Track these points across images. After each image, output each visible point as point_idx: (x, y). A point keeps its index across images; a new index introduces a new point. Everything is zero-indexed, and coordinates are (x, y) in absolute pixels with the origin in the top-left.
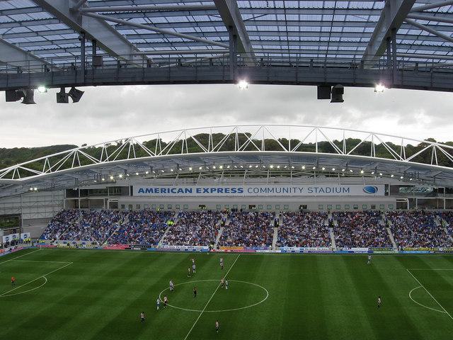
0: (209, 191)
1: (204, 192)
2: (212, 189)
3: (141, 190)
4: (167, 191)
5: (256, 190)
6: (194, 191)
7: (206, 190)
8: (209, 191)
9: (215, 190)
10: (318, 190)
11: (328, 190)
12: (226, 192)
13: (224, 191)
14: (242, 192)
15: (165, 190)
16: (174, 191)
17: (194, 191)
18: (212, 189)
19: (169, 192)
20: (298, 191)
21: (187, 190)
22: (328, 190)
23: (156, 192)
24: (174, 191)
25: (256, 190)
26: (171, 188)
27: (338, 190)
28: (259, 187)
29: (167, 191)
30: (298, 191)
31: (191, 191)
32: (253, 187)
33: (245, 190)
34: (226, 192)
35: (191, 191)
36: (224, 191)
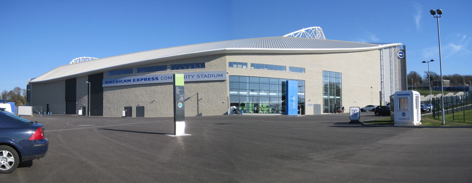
0: (140, 80)
1: (137, 81)
2: (141, 79)
3: (107, 83)
4: (118, 82)
5: (166, 78)
6: (132, 80)
7: (138, 80)
8: (140, 80)
9: (143, 79)
10: (203, 76)
11: (209, 76)
12: (149, 80)
13: (147, 80)
14: (158, 79)
15: (118, 81)
16: (122, 81)
17: (132, 80)
18: (141, 79)
19: (119, 82)
20: (191, 77)
21: (128, 80)
22: (209, 76)
23: (113, 83)
24: (122, 81)
25: (166, 78)
26: (120, 80)
27: (216, 76)
29: (118, 82)
30: (191, 77)
31: (130, 81)
34: (149, 80)
35: (130, 81)
36: (147, 80)
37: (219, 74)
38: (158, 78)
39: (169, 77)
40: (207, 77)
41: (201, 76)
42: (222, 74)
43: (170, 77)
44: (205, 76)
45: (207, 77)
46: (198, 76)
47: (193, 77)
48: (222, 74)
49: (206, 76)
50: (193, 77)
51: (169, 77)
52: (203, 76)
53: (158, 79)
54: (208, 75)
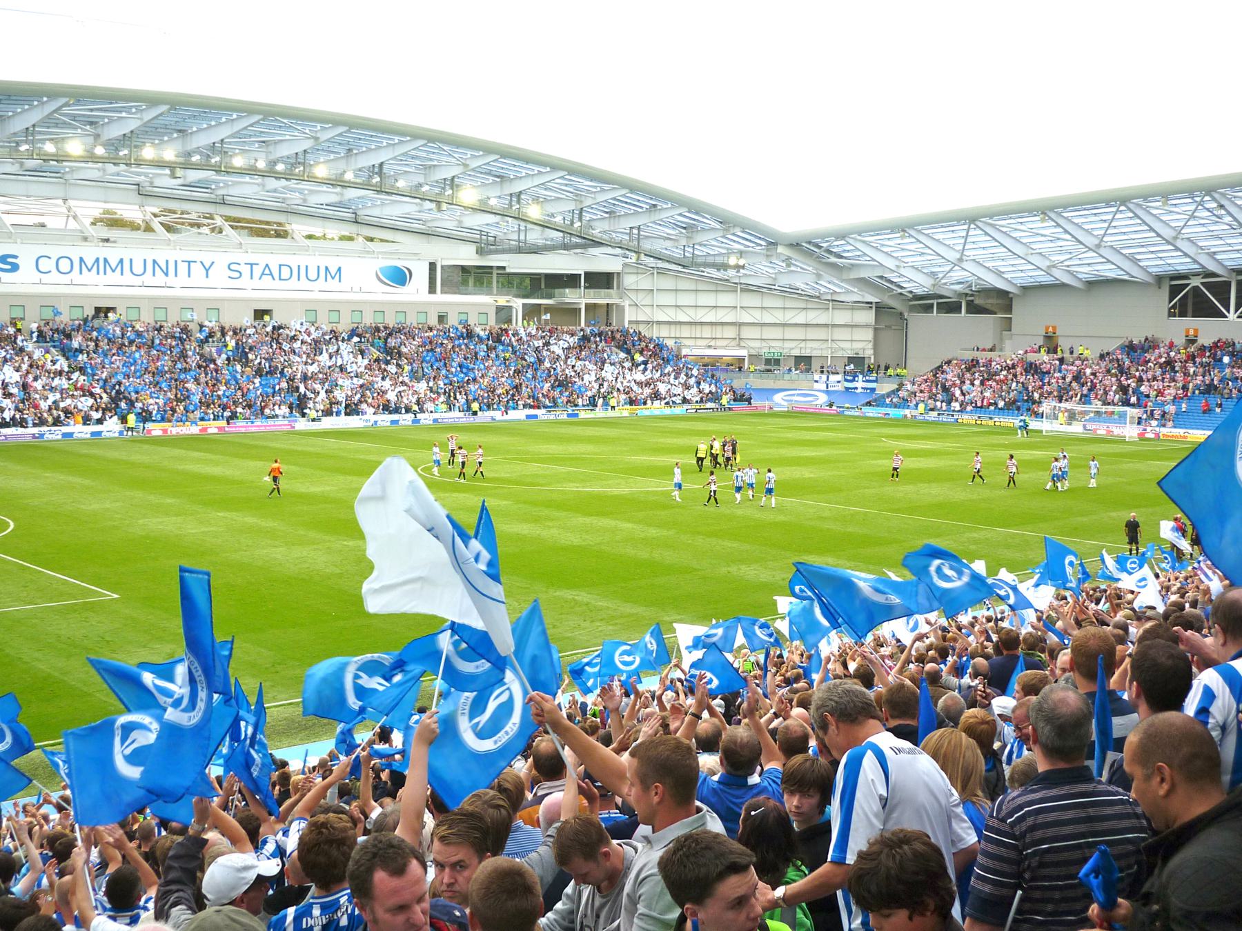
5: (65, 265)
10: (257, 271)
11: (285, 272)
14: (15, 268)
22: (285, 272)
25: (65, 265)
28: (75, 254)
32: (54, 252)
33: (26, 263)
37: (327, 268)
38: (16, 257)
39: (81, 260)
40: (276, 275)
41: (246, 270)
42: (339, 269)
43: (114, 263)
44: (267, 271)
45: (276, 275)
46: (232, 267)
47: (207, 271)
48: (339, 269)
49: (271, 274)
50: (207, 271)
51: (81, 260)
52: (257, 271)
53: (15, 268)
54: (280, 265)
